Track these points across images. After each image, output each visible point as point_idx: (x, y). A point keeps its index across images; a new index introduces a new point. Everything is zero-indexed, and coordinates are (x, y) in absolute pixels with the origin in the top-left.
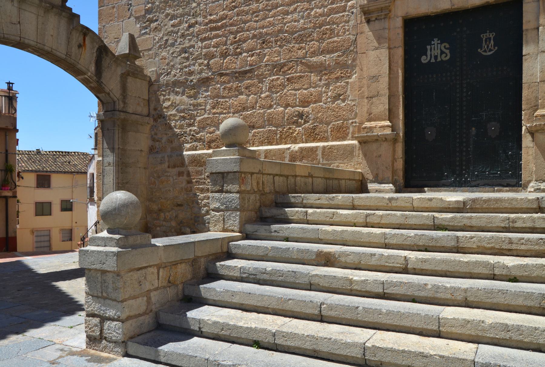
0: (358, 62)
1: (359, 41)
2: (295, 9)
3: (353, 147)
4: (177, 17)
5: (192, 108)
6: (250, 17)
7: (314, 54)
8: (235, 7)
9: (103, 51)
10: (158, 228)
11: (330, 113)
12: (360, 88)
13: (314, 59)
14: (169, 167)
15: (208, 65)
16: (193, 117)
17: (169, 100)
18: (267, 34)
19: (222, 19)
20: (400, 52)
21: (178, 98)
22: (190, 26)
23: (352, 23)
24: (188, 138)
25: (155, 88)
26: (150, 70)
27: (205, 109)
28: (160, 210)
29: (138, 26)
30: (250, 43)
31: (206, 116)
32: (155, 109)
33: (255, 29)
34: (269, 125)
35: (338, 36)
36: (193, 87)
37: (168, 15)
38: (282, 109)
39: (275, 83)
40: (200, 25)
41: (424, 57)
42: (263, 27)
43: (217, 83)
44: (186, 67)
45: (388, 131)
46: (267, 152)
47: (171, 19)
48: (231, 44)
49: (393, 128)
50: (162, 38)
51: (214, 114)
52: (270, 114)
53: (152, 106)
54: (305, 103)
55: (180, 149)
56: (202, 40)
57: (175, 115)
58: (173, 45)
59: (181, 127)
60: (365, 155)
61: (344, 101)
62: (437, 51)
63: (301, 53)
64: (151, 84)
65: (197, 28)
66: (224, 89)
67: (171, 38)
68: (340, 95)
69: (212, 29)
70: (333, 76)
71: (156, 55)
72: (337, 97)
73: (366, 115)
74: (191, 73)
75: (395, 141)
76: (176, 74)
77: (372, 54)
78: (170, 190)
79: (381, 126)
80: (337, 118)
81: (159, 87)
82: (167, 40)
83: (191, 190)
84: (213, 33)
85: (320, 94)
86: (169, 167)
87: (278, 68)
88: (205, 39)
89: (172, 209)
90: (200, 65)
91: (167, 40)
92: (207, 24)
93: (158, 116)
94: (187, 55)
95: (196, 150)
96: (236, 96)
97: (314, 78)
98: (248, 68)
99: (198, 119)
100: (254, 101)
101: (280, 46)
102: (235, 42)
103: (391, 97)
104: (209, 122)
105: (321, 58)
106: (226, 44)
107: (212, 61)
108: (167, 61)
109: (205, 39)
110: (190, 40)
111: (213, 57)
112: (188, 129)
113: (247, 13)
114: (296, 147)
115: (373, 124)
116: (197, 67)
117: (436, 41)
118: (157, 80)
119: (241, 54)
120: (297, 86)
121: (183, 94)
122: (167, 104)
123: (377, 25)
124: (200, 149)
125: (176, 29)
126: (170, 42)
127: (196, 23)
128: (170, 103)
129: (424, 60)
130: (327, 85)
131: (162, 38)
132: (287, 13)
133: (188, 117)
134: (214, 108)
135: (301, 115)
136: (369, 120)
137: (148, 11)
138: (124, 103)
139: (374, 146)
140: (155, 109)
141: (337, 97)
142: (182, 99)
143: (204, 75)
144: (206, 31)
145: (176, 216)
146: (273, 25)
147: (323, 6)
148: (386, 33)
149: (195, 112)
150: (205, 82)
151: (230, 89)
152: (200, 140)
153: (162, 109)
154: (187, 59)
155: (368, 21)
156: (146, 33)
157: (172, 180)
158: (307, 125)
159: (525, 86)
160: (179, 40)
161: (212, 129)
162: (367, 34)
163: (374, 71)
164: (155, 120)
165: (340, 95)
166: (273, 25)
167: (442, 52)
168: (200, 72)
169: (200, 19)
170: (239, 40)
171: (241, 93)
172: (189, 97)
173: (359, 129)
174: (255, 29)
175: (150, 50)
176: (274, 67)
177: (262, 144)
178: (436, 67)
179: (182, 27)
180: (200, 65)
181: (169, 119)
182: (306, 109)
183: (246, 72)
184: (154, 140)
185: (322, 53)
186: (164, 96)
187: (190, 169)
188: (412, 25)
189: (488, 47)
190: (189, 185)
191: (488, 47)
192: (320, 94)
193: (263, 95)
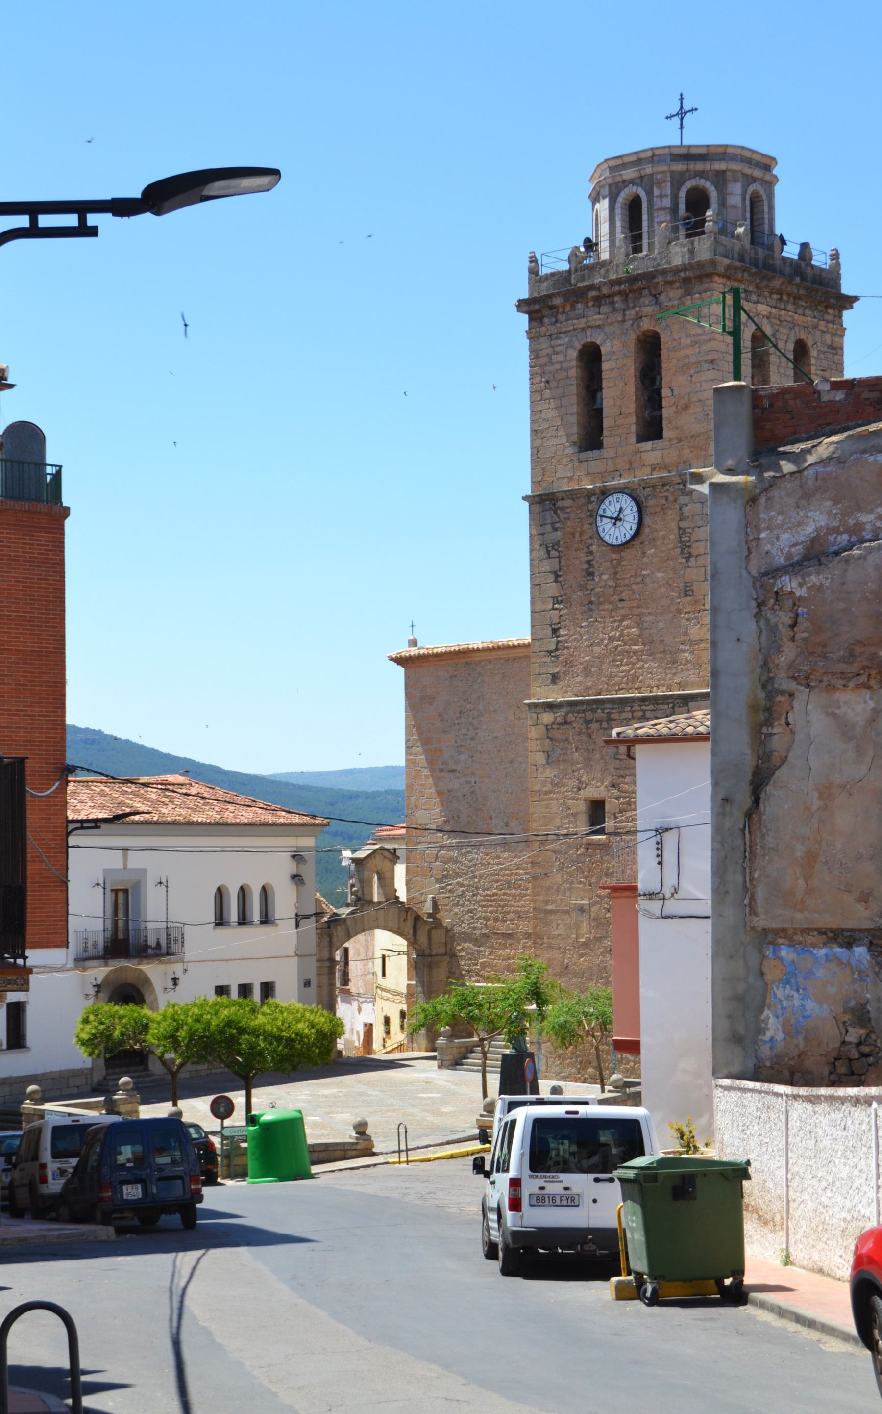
9: (417, 918)
16: (476, 959)
18: (520, 912)
22: (474, 895)
26: (447, 921)
30: (511, 915)
32: (451, 950)
42: (518, 907)
53: (448, 947)
56: (483, 906)
58: (462, 906)
59: (469, 965)
64: (447, 931)
65: (479, 897)
71: (451, 910)
74: (475, 928)
88: (483, 906)
90: (481, 923)
92: (484, 896)
93: (453, 956)
111: (489, 920)
118: (452, 930)
119: (506, 921)
122: (459, 947)
133: (473, 958)
138: (430, 949)
143: (484, 931)
144: (483, 901)
152: (481, 976)
154: (472, 918)
156: (443, 893)
164: (451, 958)
172: (475, 946)
175: (446, 905)
176: (526, 934)
180: (481, 923)
184: (450, 972)
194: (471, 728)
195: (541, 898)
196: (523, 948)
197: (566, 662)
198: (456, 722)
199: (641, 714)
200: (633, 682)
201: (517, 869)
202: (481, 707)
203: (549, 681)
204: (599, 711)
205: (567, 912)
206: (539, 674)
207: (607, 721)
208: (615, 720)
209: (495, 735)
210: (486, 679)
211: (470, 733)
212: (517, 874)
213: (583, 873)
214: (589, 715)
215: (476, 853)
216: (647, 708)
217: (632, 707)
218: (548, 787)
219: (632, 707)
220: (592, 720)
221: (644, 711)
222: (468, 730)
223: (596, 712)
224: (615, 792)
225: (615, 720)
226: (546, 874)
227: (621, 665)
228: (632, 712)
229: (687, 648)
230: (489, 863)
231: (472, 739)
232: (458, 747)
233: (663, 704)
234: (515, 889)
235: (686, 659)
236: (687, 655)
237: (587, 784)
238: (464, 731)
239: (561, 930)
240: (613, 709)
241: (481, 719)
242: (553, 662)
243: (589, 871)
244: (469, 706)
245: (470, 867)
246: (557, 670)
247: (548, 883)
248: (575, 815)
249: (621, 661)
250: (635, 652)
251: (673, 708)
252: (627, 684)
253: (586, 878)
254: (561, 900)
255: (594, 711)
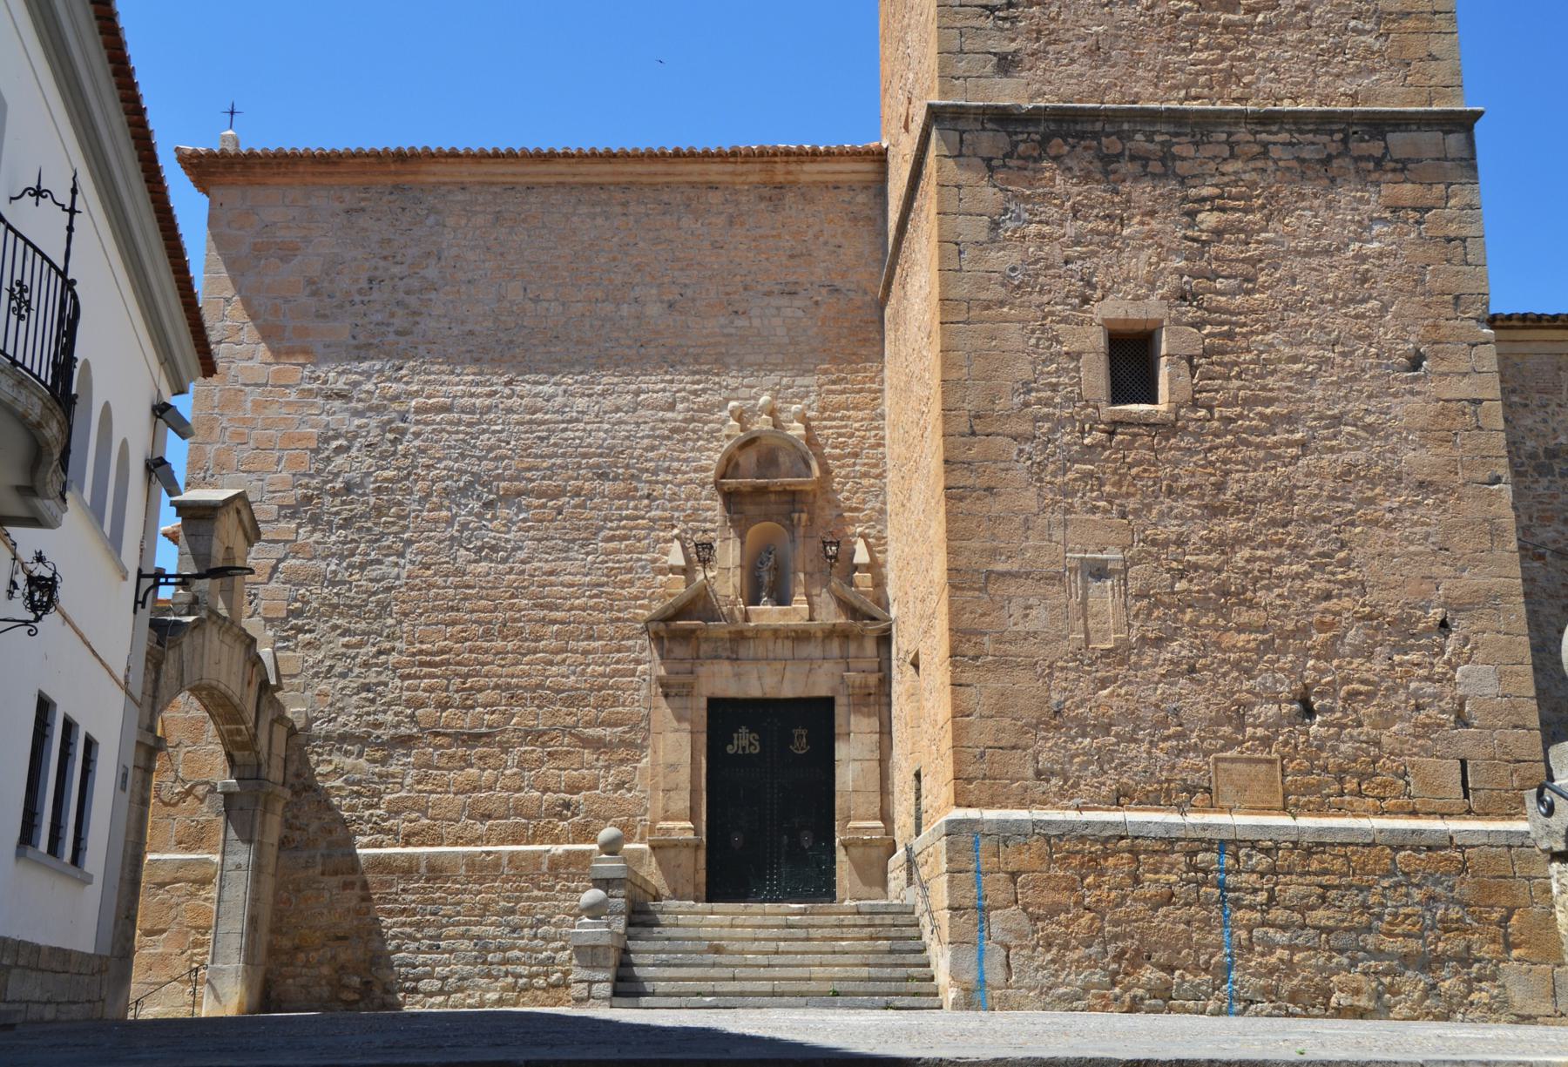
0: (650, 741)
1: (653, 717)
2: (564, 661)
3: (642, 852)
4: (355, 634)
5: (376, 779)
6: (491, 658)
7: (589, 724)
8: (467, 640)
10: (290, 981)
11: (610, 805)
12: (653, 777)
13: (590, 731)
14: (323, 874)
15: (412, 716)
17: (330, 762)
18: (518, 687)
19: (442, 652)
20: (703, 739)
21: (350, 761)
22: (380, 653)
23: (643, 692)
24: (366, 828)
25: (302, 740)
27: (402, 784)
28: (297, 949)
29: (271, 633)
31: (403, 794)
33: (500, 676)
34: (517, 815)
35: (624, 705)
36: (381, 745)
37: (335, 627)
38: (537, 794)
39: (528, 756)
40: (400, 653)
41: (729, 747)
42: (513, 676)
43: (429, 745)
44: (368, 714)
45: (690, 835)
46: (512, 854)
47: (343, 635)
48: (457, 691)
49: (696, 832)
50: (322, 661)
51: (420, 791)
52: (518, 800)
53: (292, 769)
54: (574, 789)
55: (349, 843)
56: (403, 678)
57: (339, 788)
58: (343, 675)
60: (660, 863)
61: (629, 790)
62: (744, 741)
63: (570, 720)
64: (292, 732)
65: (394, 658)
66: (441, 755)
67: (340, 664)
68: (624, 783)
69: (422, 664)
70: (615, 757)
71: (307, 686)
72: (620, 786)
73: (661, 813)
74: (377, 725)
75: (697, 847)
76: (347, 722)
77: (671, 737)
78: (322, 914)
79: (680, 828)
80: (621, 813)
81: (310, 739)
82: (332, 667)
83: (368, 912)
84: (426, 670)
85: (597, 778)
86: (323, 874)
87: (533, 735)
88: (409, 676)
89: (324, 945)
90: (396, 714)
91: (332, 667)
92: (414, 655)
93: (304, 787)
94: (371, 695)
95: (380, 846)
96: (462, 769)
97: (588, 755)
98: (484, 730)
99: (388, 797)
100: (492, 779)
101: (538, 707)
102: (464, 690)
103: (694, 792)
104: (409, 803)
105: (599, 731)
106: (447, 689)
107: (419, 712)
108: (329, 700)
109: (409, 676)
110: (379, 673)
111: (423, 705)
112: (367, 813)
113: (486, 652)
114: (559, 849)
115: (670, 824)
116: (389, 717)
117: (743, 730)
119: (473, 707)
120: (562, 764)
121: (360, 755)
123: (678, 702)
124: (388, 846)
125: (352, 652)
126: (338, 669)
127: (393, 649)
128: (331, 767)
129: (730, 749)
130: (608, 768)
131: (322, 661)
132: (551, 663)
134: (419, 783)
135: (567, 805)
136: (666, 819)
137: (297, 614)
139: (672, 853)
140: (298, 776)
141: (620, 786)
142: (359, 764)
143: (403, 730)
145: (334, 958)
146: (529, 675)
147: (603, 663)
148: (688, 714)
149: (382, 787)
150: (406, 742)
151: (451, 757)
153: (313, 776)
154: (373, 701)
155: (666, 696)
156: (287, 648)
157: (327, 895)
158: (576, 819)
159: (838, 794)
160: (357, 670)
161: (414, 816)
162: (664, 710)
163: (672, 759)
164: (296, 793)
165: (624, 783)
166: (529, 675)
167: (751, 744)
168: (397, 726)
169: (398, 644)
170: (471, 688)
171: (471, 765)
172: (374, 761)
173: (652, 830)
174: (500, 676)
175: (295, 676)
176: (527, 733)
177: (502, 842)
178: (743, 760)
179: (363, 651)
180: (396, 714)
181: (329, 795)
182: (575, 797)
183: (481, 735)
185: (601, 724)
186: (319, 754)
187: (370, 877)
188: (715, 705)
189: (800, 747)
190: (364, 904)
191: (800, 747)
192: (597, 778)
193: (508, 772)
194: (400, 312)
195: (975, 544)
196: (520, 765)
197: (1039, 32)
198: (357, 298)
199: (1256, 149)
200: (1224, 84)
201: (513, 596)
202: (432, 272)
203: (989, 69)
204: (1138, 137)
205: (1056, 578)
206: (961, 51)
207: (1163, 160)
208: (1183, 159)
209: (468, 327)
210: (450, 221)
211: (396, 321)
212: (512, 607)
213: (1101, 485)
214: (1112, 145)
215: (397, 564)
216: (1272, 138)
217: (1230, 134)
218: (1002, 293)
219: (1230, 134)
220: (1121, 154)
221: (1265, 145)
222: (392, 315)
223: (1131, 139)
224: (1191, 313)
225: (1183, 159)
226: (989, 489)
227: (1192, 51)
228: (1231, 146)
229: (1367, 27)
230: (430, 586)
231: (398, 333)
232: (357, 347)
233: (1315, 132)
234: (505, 638)
235: (1368, 49)
236: (1369, 39)
237: (1107, 292)
238: (379, 317)
239: (1039, 619)
240: (1177, 135)
241: (433, 295)
242: (1002, 30)
243: (1119, 484)
244: (396, 270)
245: (375, 593)
246: (1013, 46)
247: (997, 507)
248: (1075, 356)
249: (1193, 40)
250: (1227, 27)
251: (1345, 141)
252: (1211, 89)
253: (1110, 499)
254: (1037, 549)
255: (1122, 136)
